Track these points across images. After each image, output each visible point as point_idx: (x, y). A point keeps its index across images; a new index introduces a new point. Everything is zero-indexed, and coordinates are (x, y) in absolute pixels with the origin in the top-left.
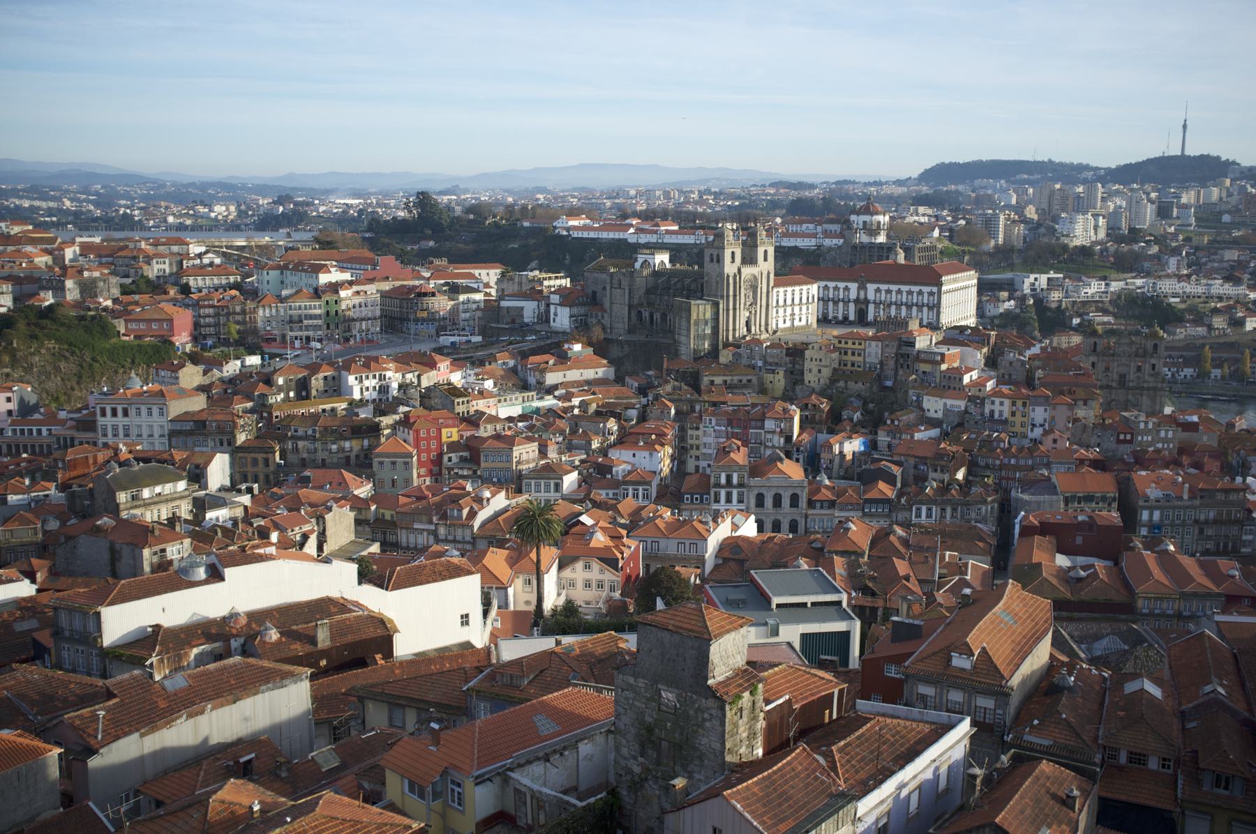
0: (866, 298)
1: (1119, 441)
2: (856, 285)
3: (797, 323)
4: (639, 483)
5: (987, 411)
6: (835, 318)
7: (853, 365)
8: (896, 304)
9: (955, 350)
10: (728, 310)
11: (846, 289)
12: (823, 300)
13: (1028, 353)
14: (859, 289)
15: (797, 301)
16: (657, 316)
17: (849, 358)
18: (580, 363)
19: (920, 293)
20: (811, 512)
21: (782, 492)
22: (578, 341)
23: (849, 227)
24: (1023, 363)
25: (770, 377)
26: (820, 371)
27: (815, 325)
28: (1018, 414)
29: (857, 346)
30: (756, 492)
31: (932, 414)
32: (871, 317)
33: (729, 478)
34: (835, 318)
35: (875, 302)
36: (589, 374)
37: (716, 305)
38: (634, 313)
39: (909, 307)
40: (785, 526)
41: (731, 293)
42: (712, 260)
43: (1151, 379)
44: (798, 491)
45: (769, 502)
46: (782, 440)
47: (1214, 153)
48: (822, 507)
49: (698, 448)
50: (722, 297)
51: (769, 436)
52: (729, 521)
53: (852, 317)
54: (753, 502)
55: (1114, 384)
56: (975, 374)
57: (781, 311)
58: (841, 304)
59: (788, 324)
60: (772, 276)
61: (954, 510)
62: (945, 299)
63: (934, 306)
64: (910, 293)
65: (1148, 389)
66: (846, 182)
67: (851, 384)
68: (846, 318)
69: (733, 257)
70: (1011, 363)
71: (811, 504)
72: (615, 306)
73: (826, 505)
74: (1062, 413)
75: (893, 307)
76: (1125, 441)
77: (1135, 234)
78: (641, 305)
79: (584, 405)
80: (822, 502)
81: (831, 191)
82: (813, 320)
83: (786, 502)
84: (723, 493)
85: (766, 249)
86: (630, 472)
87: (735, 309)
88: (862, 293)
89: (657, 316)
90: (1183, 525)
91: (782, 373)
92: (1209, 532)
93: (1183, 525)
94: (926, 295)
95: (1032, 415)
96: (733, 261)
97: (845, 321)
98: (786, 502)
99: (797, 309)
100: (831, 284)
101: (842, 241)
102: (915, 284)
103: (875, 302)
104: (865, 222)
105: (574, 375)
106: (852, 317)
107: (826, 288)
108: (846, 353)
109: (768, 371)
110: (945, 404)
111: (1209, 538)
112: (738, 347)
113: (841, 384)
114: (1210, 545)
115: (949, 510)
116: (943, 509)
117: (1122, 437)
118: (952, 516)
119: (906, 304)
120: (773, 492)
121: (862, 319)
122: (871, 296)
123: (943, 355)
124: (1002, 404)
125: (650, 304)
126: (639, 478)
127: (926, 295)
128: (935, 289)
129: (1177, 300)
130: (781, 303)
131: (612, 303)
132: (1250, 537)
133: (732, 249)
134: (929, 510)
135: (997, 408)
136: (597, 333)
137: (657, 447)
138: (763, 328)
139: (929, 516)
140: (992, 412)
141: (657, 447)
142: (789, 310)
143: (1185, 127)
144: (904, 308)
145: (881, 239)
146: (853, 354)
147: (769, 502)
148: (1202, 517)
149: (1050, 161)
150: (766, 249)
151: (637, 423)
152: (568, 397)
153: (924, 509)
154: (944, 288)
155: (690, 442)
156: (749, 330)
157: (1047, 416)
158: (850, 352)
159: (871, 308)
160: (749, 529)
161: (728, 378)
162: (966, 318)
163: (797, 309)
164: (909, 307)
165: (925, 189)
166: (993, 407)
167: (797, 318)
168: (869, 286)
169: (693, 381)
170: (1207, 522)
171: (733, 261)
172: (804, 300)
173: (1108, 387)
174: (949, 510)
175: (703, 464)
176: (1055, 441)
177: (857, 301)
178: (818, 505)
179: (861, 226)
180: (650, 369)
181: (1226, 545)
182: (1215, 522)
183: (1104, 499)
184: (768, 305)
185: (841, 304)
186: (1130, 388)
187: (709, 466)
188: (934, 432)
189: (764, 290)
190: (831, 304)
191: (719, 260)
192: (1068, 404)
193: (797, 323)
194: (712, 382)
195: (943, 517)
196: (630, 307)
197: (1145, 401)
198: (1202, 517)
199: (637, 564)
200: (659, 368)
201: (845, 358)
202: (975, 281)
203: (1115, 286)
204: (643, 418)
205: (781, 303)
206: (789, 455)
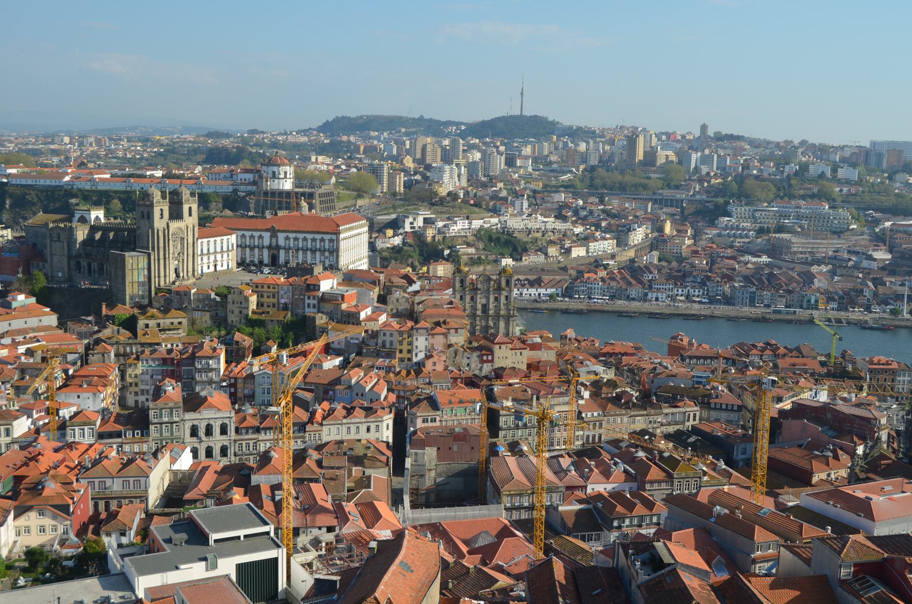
0: (277, 245)
1: (483, 362)
2: (269, 234)
4: (85, 424)
5: (380, 341)
9: (351, 292)
10: (159, 259)
11: (261, 237)
12: (241, 246)
13: (411, 289)
14: (271, 237)
15: (218, 250)
16: (95, 266)
17: (265, 300)
18: (25, 311)
19: (322, 240)
21: (212, 422)
22: (21, 291)
23: (261, 177)
24: (407, 300)
26: (241, 312)
27: (235, 270)
28: (405, 343)
29: (271, 290)
30: (188, 425)
35: (284, 248)
36: (33, 322)
37: (149, 255)
38: (73, 263)
39: (313, 251)
41: (161, 245)
42: (143, 217)
44: (227, 421)
48: (247, 433)
49: (136, 385)
50: (153, 249)
52: (167, 456)
53: (266, 260)
56: (369, 311)
57: (205, 258)
58: (256, 250)
60: (196, 229)
62: (343, 245)
63: (334, 251)
64: (314, 240)
71: (237, 430)
72: (56, 259)
73: (250, 431)
74: (439, 342)
76: (488, 361)
78: (78, 256)
79: (30, 353)
80: (247, 429)
82: (233, 265)
83: (217, 430)
85: (190, 205)
86: (76, 414)
89: (95, 266)
95: (415, 343)
96: (162, 217)
99: (219, 257)
100: (248, 234)
101: (255, 188)
102: (318, 233)
105: (17, 324)
106: (266, 260)
107: (243, 236)
108: (262, 296)
112: (169, 291)
117: (485, 358)
122: (281, 242)
123: (343, 296)
124: (391, 335)
125: (88, 255)
127: (327, 242)
128: (334, 237)
130: (205, 251)
131: (52, 255)
133: (161, 208)
135: (388, 339)
136: (41, 282)
137: (99, 388)
138: (190, 274)
140: (384, 343)
141: (99, 388)
142: (212, 258)
144: (309, 252)
145: (287, 185)
150: (190, 205)
151: (82, 365)
152: (15, 344)
154: (342, 236)
156: (178, 276)
157: (426, 343)
159: (282, 253)
160: (185, 462)
161: (161, 321)
162: (360, 259)
163: (219, 257)
164: (313, 251)
167: (219, 263)
168: (279, 234)
169: (130, 324)
171: (162, 217)
172: (225, 249)
175: (142, 398)
176: (435, 364)
177: (270, 247)
178: (244, 431)
179: (270, 175)
180: (89, 315)
184: (194, 254)
185: (256, 250)
187: (147, 400)
188: (337, 361)
189: (191, 241)
190: (248, 250)
191: (149, 216)
192: (443, 334)
193: (219, 268)
194: (147, 326)
196: (70, 257)
199: (86, 506)
200: (98, 313)
201: (262, 300)
202: (366, 228)
204: (84, 360)
205: (205, 251)
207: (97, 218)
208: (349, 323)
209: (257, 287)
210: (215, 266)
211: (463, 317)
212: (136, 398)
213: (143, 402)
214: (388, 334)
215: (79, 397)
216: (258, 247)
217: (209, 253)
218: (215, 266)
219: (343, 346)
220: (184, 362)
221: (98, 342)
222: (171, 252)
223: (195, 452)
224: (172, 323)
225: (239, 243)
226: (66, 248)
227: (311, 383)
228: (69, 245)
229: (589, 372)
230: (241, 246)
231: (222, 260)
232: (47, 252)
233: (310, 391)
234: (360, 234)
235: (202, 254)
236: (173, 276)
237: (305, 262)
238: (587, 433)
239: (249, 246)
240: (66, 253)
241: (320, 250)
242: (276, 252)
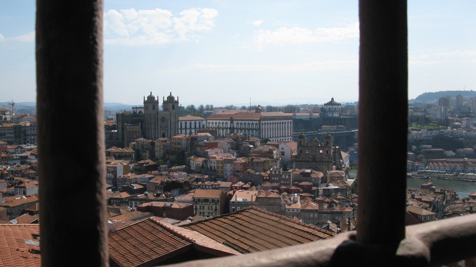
11: (226, 123)
14: (231, 123)
55: (310, 160)
67: (170, 156)
88: (232, 125)
124: (214, 163)
129: (463, 139)
142: (188, 131)
157: (232, 168)
166: (211, 165)
173: (308, 161)
222: (159, 126)
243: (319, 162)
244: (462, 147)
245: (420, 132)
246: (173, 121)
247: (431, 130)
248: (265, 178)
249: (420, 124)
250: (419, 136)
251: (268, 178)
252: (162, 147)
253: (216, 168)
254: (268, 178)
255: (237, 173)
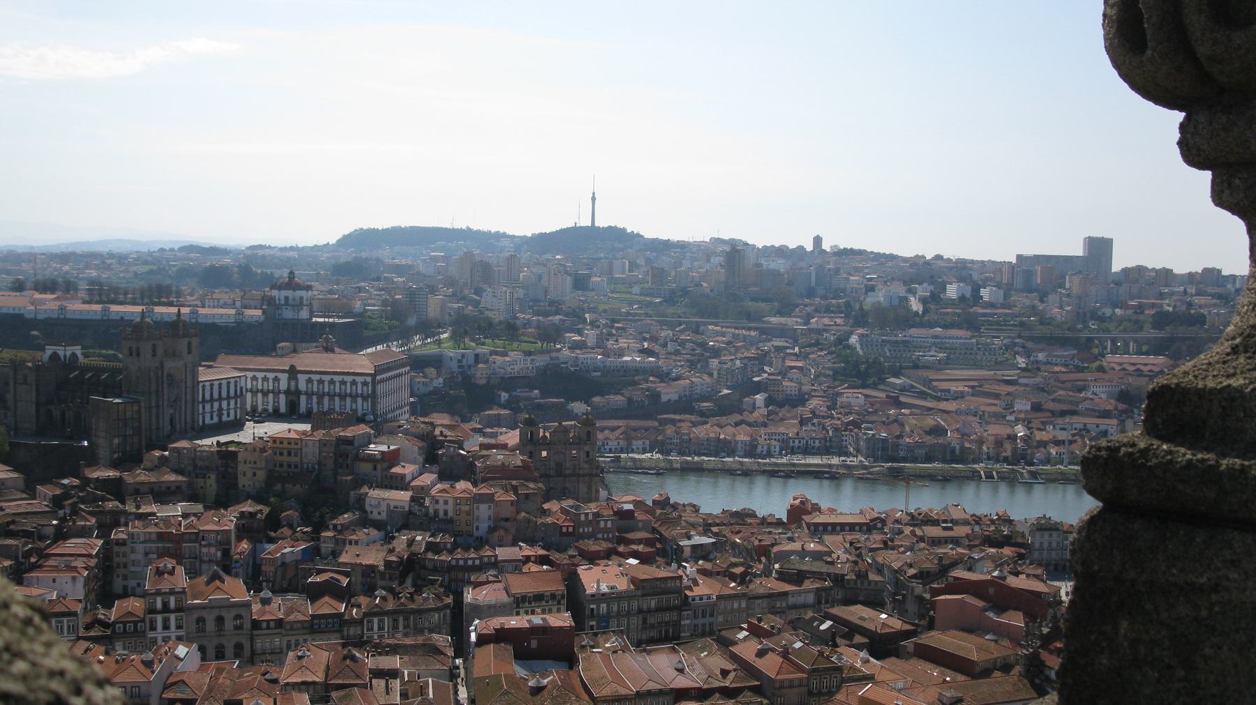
2: (286, 375)
3: (225, 418)
5: (431, 511)
6: (265, 410)
7: (289, 466)
8: (328, 394)
10: (150, 408)
11: (276, 379)
14: (289, 379)
15: (224, 394)
17: (285, 458)
19: (354, 383)
20: (256, 632)
21: (224, 613)
25: (200, 482)
26: (254, 474)
29: (293, 446)
30: (196, 615)
31: (375, 516)
32: (303, 407)
33: (165, 604)
34: (265, 410)
35: (306, 393)
40: (229, 650)
41: (153, 389)
42: (131, 354)
43: (586, 466)
44: (242, 611)
45: (211, 625)
46: (219, 554)
47: (620, 226)
48: (268, 628)
49: (125, 566)
51: (205, 550)
53: (283, 409)
54: (193, 627)
55: (552, 473)
58: (271, 395)
59: (216, 419)
61: (406, 619)
62: (380, 388)
64: (343, 383)
65: (584, 476)
66: (261, 247)
67: (288, 486)
68: (276, 410)
69: (154, 351)
70: (451, 457)
75: (326, 399)
77: (555, 306)
80: (268, 621)
81: (246, 257)
84: (159, 618)
87: (158, 406)
88: (293, 383)
90: (629, 614)
91: (213, 477)
92: (652, 620)
93: (629, 614)
94: (360, 385)
96: (154, 354)
97: (276, 416)
98: (229, 625)
99: (224, 404)
103: (306, 393)
104: (287, 298)
106: (283, 409)
107: (254, 378)
108: (281, 454)
109: (197, 477)
110: (388, 505)
111: (652, 627)
113: (278, 487)
114: (654, 633)
115: (401, 620)
116: (395, 620)
118: (405, 627)
119: (339, 395)
120: (216, 613)
121: (292, 414)
122: (302, 386)
124: (446, 503)
126: (64, 609)
127: (360, 385)
130: (208, 396)
131: (16, 401)
132: (688, 622)
134: (381, 621)
135: (441, 507)
139: (381, 628)
140: (436, 512)
142: (216, 405)
143: (594, 199)
144: (337, 399)
146: (289, 454)
147: (211, 625)
148: (645, 607)
149: (468, 228)
153: (376, 620)
154: (378, 378)
155: (116, 560)
157: (491, 512)
158: (285, 453)
159: (303, 399)
162: (400, 407)
163: (224, 404)
165: (345, 256)
166: (437, 507)
167: (225, 413)
170: (649, 611)
172: (232, 393)
174: (401, 620)
177: (288, 392)
180: (64, 478)
181: (667, 632)
182: (659, 609)
183: (553, 596)
184: (193, 401)
185: (271, 395)
186: (566, 476)
190: (260, 395)
193: (225, 418)
195: (395, 628)
196: (38, 404)
197: (583, 488)
198: (645, 607)
203: (541, 361)
206: (227, 570)
207: (74, 355)
208: (391, 488)
209: (274, 442)
210: (220, 415)
211: (535, 481)
212: (125, 583)
213: (133, 588)
214: (441, 501)
215: (54, 581)
216: (273, 392)
217: (212, 400)
218: (220, 415)
219: (384, 516)
220: (186, 537)
221: (75, 512)
223: (202, 649)
224: (169, 488)
225: (249, 386)
226: (34, 394)
227: (345, 564)
228: (37, 390)
229: (694, 547)
230: (251, 391)
231: (228, 409)
232: (10, 397)
233: (346, 574)
234: (400, 375)
235: (204, 401)
236: (167, 428)
237: (331, 411)
238: (695, 622)
239: (262, 391)
240: (34, 399)
241: (351, 395)
242: (295, 398)
243: (570, 476)
244: (602, 395)
245: (508, 359)
246: (189, 383)
247: (529, 353)
248: (564, 530)
249: (498, 337)
250: (509, 369)
251: (571, 530)
252: (263, 465)
253: (450, 514)
254: (571, 530)
255: (503, 524)
